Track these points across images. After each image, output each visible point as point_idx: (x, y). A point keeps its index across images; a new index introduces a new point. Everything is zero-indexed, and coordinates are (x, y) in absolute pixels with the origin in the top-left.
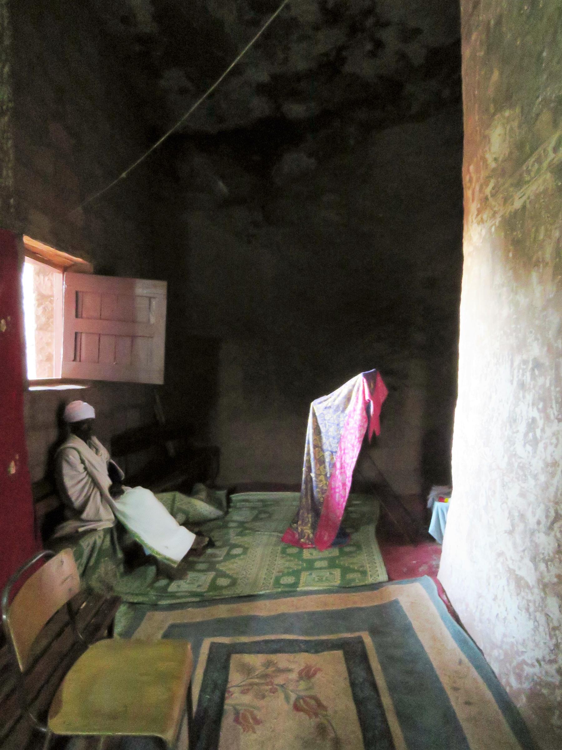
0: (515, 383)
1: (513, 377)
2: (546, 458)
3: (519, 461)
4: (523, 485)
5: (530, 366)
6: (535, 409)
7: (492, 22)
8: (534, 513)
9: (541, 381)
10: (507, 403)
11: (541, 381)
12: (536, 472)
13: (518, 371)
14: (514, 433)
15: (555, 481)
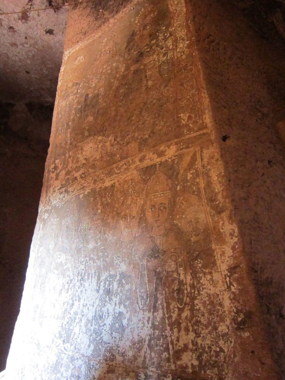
0: (101, 291)
1: (99, 287)
2: (133, 338)
3: (106, 346)
4: (110, 363)
5: (118, 277)
6: (122, 306)
7: (90, 95)
10: (93, 306)
12: (123, 351)
13: (105, 283)
14: (100, 326)
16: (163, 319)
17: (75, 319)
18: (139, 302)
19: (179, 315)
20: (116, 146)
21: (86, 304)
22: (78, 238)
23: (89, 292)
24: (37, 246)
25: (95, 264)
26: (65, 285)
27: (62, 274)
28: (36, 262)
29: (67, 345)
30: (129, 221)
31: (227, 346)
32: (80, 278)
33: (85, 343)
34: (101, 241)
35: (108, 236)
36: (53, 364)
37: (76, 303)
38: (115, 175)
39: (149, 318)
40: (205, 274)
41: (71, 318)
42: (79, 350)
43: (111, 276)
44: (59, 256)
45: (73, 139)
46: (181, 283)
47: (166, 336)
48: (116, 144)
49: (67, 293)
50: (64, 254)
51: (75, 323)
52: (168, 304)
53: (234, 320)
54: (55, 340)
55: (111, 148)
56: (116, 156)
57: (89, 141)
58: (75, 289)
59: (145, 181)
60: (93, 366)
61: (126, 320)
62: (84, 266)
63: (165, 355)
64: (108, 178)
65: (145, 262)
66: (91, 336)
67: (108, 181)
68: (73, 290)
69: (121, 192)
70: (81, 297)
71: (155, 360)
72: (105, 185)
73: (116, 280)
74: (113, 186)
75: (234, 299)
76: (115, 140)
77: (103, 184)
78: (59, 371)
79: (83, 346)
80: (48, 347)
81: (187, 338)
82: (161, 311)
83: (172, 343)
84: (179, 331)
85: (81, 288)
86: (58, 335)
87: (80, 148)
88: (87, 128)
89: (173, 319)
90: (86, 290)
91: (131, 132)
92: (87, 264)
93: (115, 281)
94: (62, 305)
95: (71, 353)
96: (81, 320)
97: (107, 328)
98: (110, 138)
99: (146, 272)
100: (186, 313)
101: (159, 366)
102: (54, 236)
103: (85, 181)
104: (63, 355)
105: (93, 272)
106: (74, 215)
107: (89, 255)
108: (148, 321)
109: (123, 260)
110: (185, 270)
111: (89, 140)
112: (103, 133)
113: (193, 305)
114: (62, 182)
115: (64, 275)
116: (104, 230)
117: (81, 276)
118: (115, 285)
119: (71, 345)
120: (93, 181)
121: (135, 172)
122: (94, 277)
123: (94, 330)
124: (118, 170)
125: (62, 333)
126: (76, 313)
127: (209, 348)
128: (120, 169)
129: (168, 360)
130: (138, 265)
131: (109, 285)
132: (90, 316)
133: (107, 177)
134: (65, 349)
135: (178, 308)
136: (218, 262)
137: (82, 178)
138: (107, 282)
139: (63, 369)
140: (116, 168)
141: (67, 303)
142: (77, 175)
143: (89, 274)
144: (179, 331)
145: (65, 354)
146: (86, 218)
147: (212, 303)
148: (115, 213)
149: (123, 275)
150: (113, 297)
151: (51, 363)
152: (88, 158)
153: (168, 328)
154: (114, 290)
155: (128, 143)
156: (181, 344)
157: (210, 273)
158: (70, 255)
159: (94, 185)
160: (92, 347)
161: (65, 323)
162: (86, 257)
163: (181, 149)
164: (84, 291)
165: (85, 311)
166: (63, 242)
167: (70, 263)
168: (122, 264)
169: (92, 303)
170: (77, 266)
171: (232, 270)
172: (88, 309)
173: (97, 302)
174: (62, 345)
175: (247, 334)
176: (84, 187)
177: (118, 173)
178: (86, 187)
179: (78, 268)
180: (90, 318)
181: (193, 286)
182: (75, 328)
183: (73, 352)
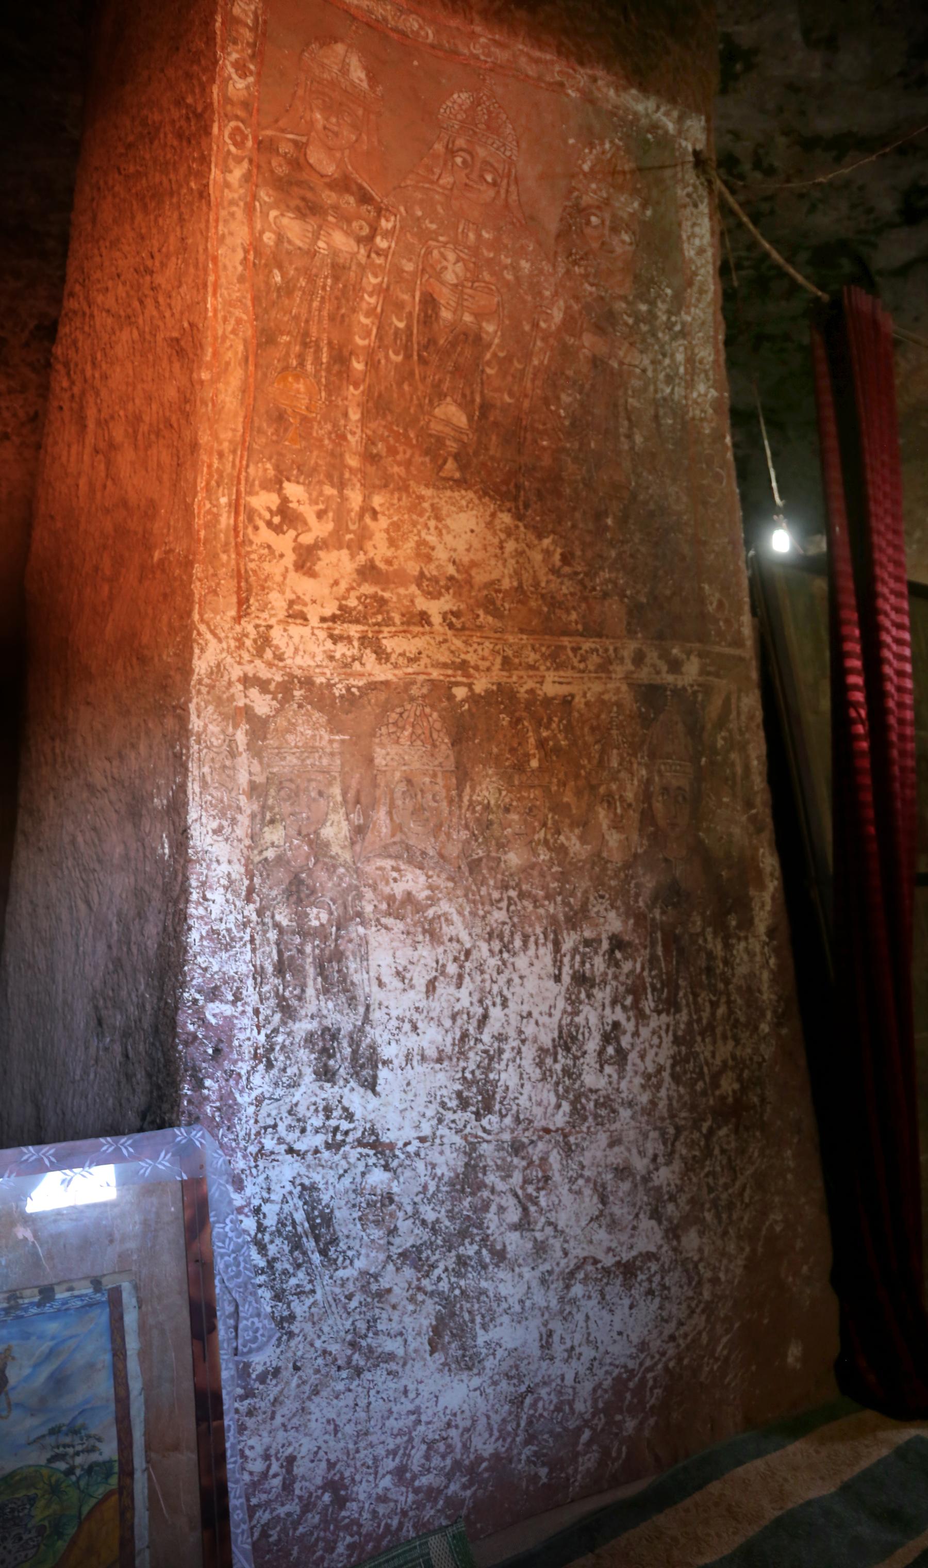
0: (566, 979)
1: (560, 969)
4: (613, 1128)
5: (605, 945)
6: (618, 1009)
8: (642, 1154)
9: (627, 966)
11: (627, 966)
13: (573, 958)
14: (576, 1058)
15: (663, 1093)
16: (689, 1024)
17: (501, 1051)
18: (650, 996)
19: (713, 1014)
20: (568, 583)
21: (530, 1014)
22: (467, 827)
23: (531, 984)
24: (244, 820)
25: (541, 911)
26: (444, 966)
27: (425, 931)
28: (257, 881)
29: (491, 1121)
30: (619, 811)
31: (767, 1051)
32: (496, 945)
33: (545, 1103)
34: (549, 849)
35: (568, 839)
36: (457, 1176)
37: (496, 1013)
38: (570, 673)
39: (668, 1025)
40: (739, 939)
41: (486, 1052)
42: (531, 1122)
43: (587, 943)
44: (395, 874)
46: (710, 956)
47: (698, 1054)
49: (459, 986)
50: (418, 872)
51: (503, 1063)
52: (695, 995)
53: (775, 1012)
54: (449, 1116)
55: (551, 577)
56: (568, 613)
57: (464, 503)
58: (487, 976)
59: (646, 721)
60: (577, 1145)
61: (629, 1035)
62: (504, 912)
63: (700, 1086)
64: (552, 673)
65: (657, 913)
66: (557, 1084)
68: (478, 978)
69: (593, 729)
70: (509, 996)
71: (687, 1098)
73: (601, 952)
74: (567, 702)
75: (776, 979)
76: (565, 559)
78: (482, 1185)
79: (538, 1111)
80: (422, 1140)
81: (725, 1050)
82: (685, 1011)
83: (707, 1064)
84: (714, 1042)
85: (507, 972)
86: (453, 1104)
87: (426, 505)
88: (452, 446)
89: (705, 1022)
90: (521, 977)
92: (512, 908)
93: (596, 953)
94: (448, 1023)
95: (506, 1136)
96: (519, 1052)
97: (591, 1059)
98: (546, 542)
99: (659, 935)
100: (721, 1011)
101: (693, 1108)
102: (339, 798)
103: (465, 642)
104: (485, 1145)
105: (539, 930)
106: (434, 746)
107: (518, 885)
108: (667, 1031)
109: (612, 906)
110: (715, 933)
111: (463, 497)
112: (517, 508)
113: (728, 995)
114: (345, 598)
115: (434, 936)
116: (555, 823)
117: (502, 940)
118: (599, 963)
119: (502, 1116)
120: (499, 660)
121: (624, 688)
122: (544, 944)
123: (563, 1070)
125: (465, 1094)
126: (501, 1038)
127: (751, 1059)
128: (583, 660)
129: (704, 1093)
130: (645, 917)
131: (583, 963)
132: (546, 1040)
133: (548, 669)
134: (484, 1130)
135: (711, 1002)
136: (756, 920)
137: (451, 626)
138: (578, 958)
139: (491, 1178)
140: (575, 650)
141: (465, 1017)
142: (435, 608)
143: (525, 939)
144: (714, 1042)
145: (488, 1142)
146: (490, 772)
147: (749, 989)
148: (582, 783)
149: (617, 943)
150: (595, 991)
151: (449, 1174)
153: (699, 1039)
154: (597, 973)
155: (605, 595)
156: (718, 1061)
157: (746, 938)
158: (444, 876)
160: (566, 1107)
161: (472, 1066)
162: (506, 887)
163: (709, 674)
164: (517, 980)
165: (530, 1029)
166: (397, 828)
167: (450, 900)
168: (612, 914)
169: (545, 1008)
170: (481, 913)
171: (771, 932)
172: (537, 1023)
173: (561, 1004)
174: (474, 1123)
175: (784, 1031)
176: (464, 662)
178: (476, 668)
179: (484, 917)
180: (548, 1044)
181: (726, 962)
182: (504, 1076)
183: (513, 1131)
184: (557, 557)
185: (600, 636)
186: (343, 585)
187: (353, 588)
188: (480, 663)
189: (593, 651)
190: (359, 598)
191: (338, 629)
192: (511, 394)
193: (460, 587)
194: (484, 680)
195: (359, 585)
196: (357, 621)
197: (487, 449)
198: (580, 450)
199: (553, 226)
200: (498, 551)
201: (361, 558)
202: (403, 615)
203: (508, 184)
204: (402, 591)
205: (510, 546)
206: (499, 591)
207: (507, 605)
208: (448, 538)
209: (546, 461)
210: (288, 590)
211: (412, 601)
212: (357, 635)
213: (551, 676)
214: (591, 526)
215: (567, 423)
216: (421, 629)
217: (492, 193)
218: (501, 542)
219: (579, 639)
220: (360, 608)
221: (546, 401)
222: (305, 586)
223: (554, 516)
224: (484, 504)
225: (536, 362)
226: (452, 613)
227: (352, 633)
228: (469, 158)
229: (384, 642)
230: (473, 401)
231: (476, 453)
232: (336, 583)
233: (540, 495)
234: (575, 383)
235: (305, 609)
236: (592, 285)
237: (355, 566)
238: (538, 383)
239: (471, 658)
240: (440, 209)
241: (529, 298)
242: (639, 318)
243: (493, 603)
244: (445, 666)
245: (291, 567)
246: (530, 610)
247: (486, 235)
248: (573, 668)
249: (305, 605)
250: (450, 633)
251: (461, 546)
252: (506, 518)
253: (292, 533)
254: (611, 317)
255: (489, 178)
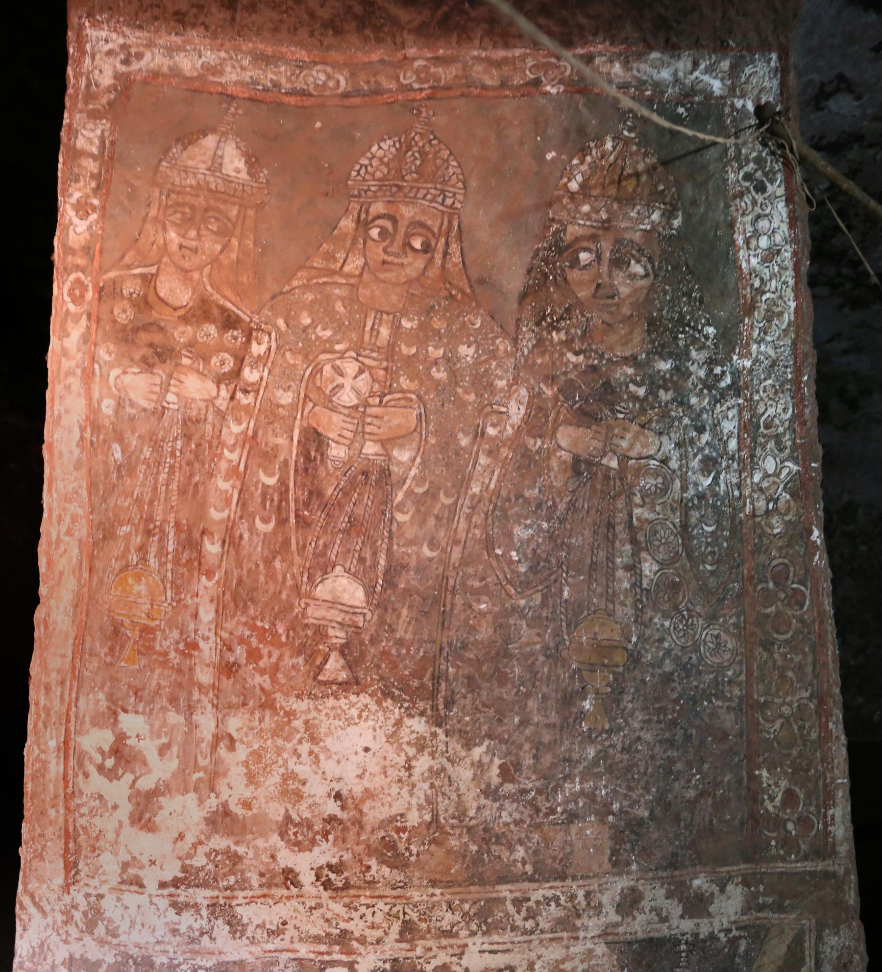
20: (509, 806)
38: (509, 936)
45: (240, 652)
48: (512, 798)
55: (483, 801)
56: (511, 848)
57: (354, 712)
64: (478, 939)
67: (478, 948)
72: (465, 962)
76: (506, 773)
77: (455, 959)
87: (298, 724)
91: (581, 768)
98: (478, 752)
103: (347, 906)
111: (352, 705)
112: (435, 708)
114: (189, 856)
120: (396, 927)
124: (526, 919)
133: (473, 934)
137: (327, 885)
140: (517, 903)
152: (345, 792)
155: (572, 817)
159: (404, 945)
176: (344, 933)
177: (525, 932)
178: (362, 940)
184: (495, 771)
185: (563, 878)
186: (190, 839)
187: (201, 843)
188: (368, 932)
189: (548, 901)
190: (208, 855)
191: (183, 894)
192: (432, 545)
193: (345, 829)
194: (372, 957)
195: (208, 838)
196: (205, 885)
197: (392, 630)
198: (544, 604)
199: (514, 281)
200: (404, 774)
201: (213, 803)
202: (262, 875)
203: (447, 244)
204: (260, 843)
205: (423, 764)
206: (404, 830)
207: (414, 849)
208: (328, 766)
209: (485, 632)
210: (122, 849)
211: (273, 857)
212: (206, 902)
213: (476, 944)
214: (554, 717)
215: (522, 569)
216: (285, 892)
217: (420, 263)
218: (409, 760)
219: (526, 885)
220: (210, 867)
221: (489, 544)
222: (143, 844)
223: (491, 712)
224: (385, 710)
225: (476, 489)
226: (330, 867)
227: (199, 900)
228: (388, 224)
229: (239, 910)
230: (375, 565)
231: (373, 641)
232: (181, 837)
233: (471, 684)
234: (539, 506)
235: (141, 873)
236: (577, 353)
237: (204, 813)
238: (477, 519)
239: (356, 927)
240: (339, 307)
241: (472, 397)
242: (655, 383)
243: (392, 846)
244: (317, 939)
245: (126, 821)
246: (449, 852)
247: (406, 324)
248: (514, 928)
249: (142, 867)
250: (325, 895)
251: (350, 772)
252: (418, 725)
253: (129, 777)
254: (609, 393)
255: (417, 244)
